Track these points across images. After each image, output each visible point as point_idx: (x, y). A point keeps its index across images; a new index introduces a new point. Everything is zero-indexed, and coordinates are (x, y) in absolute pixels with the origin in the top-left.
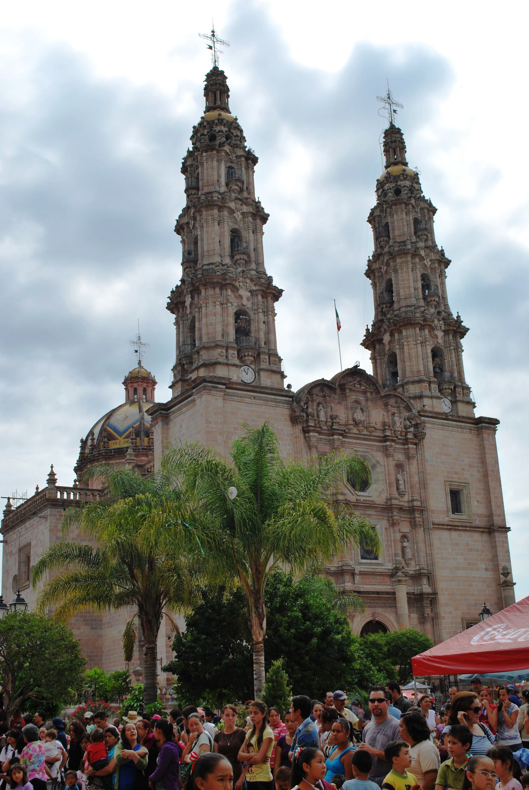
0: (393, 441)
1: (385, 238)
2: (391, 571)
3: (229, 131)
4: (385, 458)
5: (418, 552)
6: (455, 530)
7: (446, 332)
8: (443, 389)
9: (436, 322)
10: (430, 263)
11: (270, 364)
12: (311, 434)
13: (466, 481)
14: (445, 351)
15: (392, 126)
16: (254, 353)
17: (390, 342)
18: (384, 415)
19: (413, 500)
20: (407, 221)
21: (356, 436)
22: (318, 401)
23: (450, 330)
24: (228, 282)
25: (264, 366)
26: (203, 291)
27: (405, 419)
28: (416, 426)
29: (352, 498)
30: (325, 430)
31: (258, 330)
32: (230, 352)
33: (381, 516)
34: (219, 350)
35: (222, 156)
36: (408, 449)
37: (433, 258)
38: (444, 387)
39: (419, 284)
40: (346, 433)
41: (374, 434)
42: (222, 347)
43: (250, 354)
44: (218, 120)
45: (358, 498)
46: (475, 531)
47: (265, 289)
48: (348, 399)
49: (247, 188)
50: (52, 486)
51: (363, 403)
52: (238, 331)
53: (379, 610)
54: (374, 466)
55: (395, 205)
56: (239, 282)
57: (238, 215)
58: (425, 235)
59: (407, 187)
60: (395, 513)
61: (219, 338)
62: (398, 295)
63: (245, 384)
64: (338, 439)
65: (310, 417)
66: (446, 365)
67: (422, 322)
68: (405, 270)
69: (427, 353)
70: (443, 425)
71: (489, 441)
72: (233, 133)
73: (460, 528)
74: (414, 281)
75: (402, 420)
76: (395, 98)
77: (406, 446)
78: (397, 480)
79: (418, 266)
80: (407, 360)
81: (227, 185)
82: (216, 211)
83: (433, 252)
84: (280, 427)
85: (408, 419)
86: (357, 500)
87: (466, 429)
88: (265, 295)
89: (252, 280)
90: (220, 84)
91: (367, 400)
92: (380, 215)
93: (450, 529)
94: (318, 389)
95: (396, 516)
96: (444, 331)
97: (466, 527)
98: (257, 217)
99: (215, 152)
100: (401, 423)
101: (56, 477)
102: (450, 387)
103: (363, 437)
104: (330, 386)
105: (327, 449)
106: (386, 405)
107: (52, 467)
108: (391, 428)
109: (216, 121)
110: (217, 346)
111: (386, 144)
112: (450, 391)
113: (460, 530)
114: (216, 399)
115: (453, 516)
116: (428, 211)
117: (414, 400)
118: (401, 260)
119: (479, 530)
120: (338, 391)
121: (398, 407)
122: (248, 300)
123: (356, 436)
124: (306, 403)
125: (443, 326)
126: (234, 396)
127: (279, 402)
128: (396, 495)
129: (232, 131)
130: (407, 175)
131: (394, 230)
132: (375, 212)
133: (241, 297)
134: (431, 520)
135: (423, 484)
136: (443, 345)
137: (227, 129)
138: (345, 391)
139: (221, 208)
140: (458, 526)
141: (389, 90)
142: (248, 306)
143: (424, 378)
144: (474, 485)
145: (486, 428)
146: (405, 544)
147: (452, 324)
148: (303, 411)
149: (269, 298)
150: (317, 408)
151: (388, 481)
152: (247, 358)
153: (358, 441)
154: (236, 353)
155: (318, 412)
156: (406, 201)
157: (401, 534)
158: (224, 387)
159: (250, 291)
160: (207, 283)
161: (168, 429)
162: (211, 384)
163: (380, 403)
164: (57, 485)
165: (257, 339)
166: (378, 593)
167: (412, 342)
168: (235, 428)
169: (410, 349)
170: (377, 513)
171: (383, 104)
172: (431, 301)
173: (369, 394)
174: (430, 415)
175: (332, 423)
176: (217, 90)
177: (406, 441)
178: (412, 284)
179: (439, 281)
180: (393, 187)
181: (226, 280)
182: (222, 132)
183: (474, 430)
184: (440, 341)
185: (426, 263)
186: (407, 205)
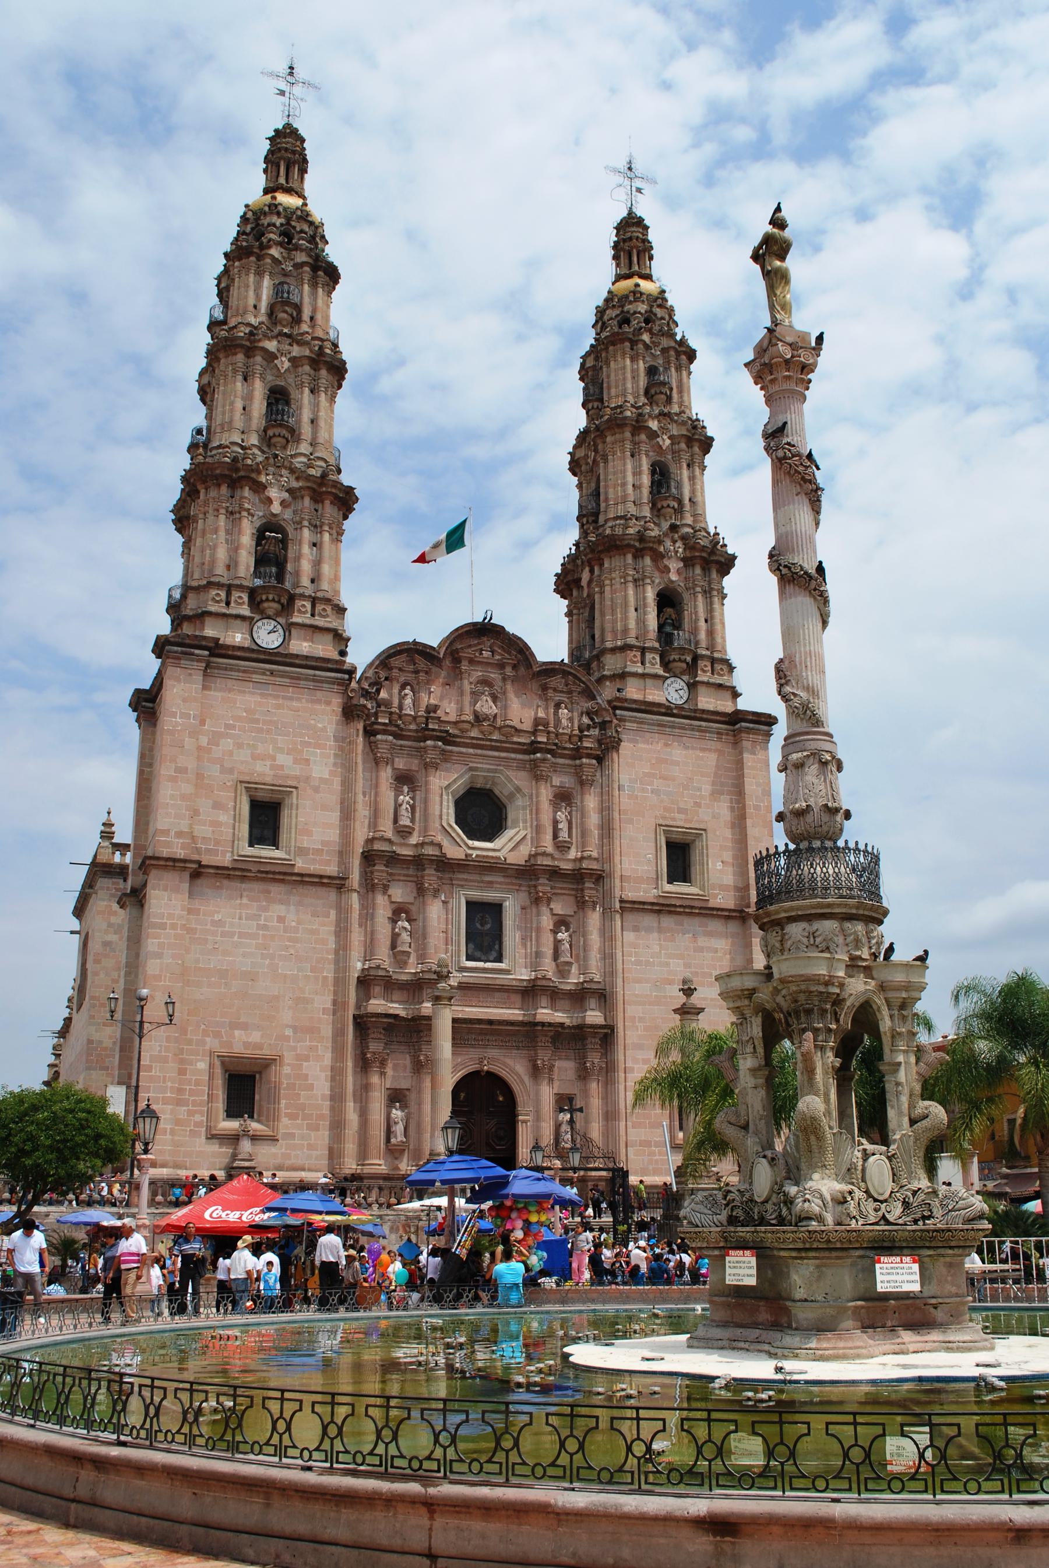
0: (549, 751)
1: (596, 404)
2: (525, 984)
3: (288, 223)
4: (534, 783)
5: (585, 950)
6: (670, 912)
7: (688, 562)
8: (669, 662)
9: (668, 543)
10: (668, 442)
11: (313, 615)
12: (379, 737)
14: (686, 596)
15: (631, 213)
16: (280, 596)
17: (590, 582)
18: (538, 706)
19: (582, 858)
20: (633, 371)
21: (475, 742)
22: (402, 679)
23: (695, 557)
24: (242, 473)
25: (297, 619)
26: (202, 492)
27: (582, 714)
28: (603, 725)
29: (454, 852)
30: (410, 730)
31: (298, 558)
32: (235, 594)
33: (513, 884)
34: (213, 592)
35: (267, 264)
37: (675, 433)
38: (672, 658)
39: (646, 480)
40: (402, 730)
41: (515, 739)
43: (271, 597)
44: (269, 206)
45: (469, 852)
46: (713, 916)
47: (314, 486)
48: (465, 675)
49: (312, 318)
50: (106, 844)
51: (498, 683)
52: (261, 561)
53: (493, 1053)
54: (511, 796)
55: (614, 344)
56: (267, 475)
57: (284, 363)
58: (661, 393)
59: (640, 313)
60: (587, 885)
61: (220, 569)
62: (607, 500)
64: (435, 747)
65: (383, 708)
66: (686, 620)
67: (637, 544)
69: (645, 598)
72: (294, 228)
73: (678, 909)
74: (634, 474)
75: (576, 714)
76: (639, 167)
77: (578, 762)
78: (555, 823)
79: (644, 447)
80: (608, 611)
81: (271, 313)
82: (240, 357)
83: (676, 422)
85: (589, 714)
87: (710, 732)
88: (317, 498)
89: (292, 470)
90: (286, 150)
91: (504, 679)
92: (594, 366)
93: (659, 912)
94: (404, 657)
95: (544, 885)
96: (683, 560)
97: (692, 907)
98: (321, 366)
99: (253, 259)
100: (571, 719)
101: (113, 829)
102: (683, 657)
103: (488, 743)
104: (429, 653)
105: (414, 764)
106: (545, 688)
107: (109, 813)
108: (552, 729)
109: (267, 209)
110: (210, 585)
111: (616, 246)
112: (684, 665)
113: (680, 913)
114: (190, 675)
115: (669, 887)
116: (678, 354)
117: (611, 682)
118: (613, 438)
119: (719, 913)
120: (447, 663)
121: (570, 692)
122: (283, 503)
123: (475, 742)
125: (680, 550)
126: (231, 670)
127: (322, 682)
128: (550, 849)
129: (293, 223)
130: (641, 294)
131: (609, 388)
132: (587, 361)
133: (269, 501)
134: (617, 893)
135: (607, 829)
136: (682, 584)
137: (283, 221)
138: (460, 662)
139: (250, 351)
140: (675, 906)
141: (631, 156)
142: (285, 517)
143: (631, 641)
145: (749, 731)
146: (560, 936)
147: (698, 546)
148: (366, 694)
149: (327, 502)
150: (400, 692)
151: (535, 823)
152: (266, 605)
153: (479, 752)
154: (245, 597)
155: (402, 698)
156: (631, 336)
157: (394, 906)
158: (206, 653)
159: (290, 491)
161: (154, 733)
162: (179, 649)
163: (534, 685)
164: (114, 841)
165: (297, 574)
166: (490, 1022)
167: (618, 579)
169: (613, 592)
170: (508, 880)
171: (620, 179)
172: (663, 507)
173: (509, 671)
174: (634, 706)
175: (427, 718)
176: (280, 158)
177: (577, 753)
178: (630, 479)
179: (685, 473)
180: (617, 316)
181: (237, 470)
182: (274, 225)
183: (727, 734)
184: (674, 577)
186: (634, 343)
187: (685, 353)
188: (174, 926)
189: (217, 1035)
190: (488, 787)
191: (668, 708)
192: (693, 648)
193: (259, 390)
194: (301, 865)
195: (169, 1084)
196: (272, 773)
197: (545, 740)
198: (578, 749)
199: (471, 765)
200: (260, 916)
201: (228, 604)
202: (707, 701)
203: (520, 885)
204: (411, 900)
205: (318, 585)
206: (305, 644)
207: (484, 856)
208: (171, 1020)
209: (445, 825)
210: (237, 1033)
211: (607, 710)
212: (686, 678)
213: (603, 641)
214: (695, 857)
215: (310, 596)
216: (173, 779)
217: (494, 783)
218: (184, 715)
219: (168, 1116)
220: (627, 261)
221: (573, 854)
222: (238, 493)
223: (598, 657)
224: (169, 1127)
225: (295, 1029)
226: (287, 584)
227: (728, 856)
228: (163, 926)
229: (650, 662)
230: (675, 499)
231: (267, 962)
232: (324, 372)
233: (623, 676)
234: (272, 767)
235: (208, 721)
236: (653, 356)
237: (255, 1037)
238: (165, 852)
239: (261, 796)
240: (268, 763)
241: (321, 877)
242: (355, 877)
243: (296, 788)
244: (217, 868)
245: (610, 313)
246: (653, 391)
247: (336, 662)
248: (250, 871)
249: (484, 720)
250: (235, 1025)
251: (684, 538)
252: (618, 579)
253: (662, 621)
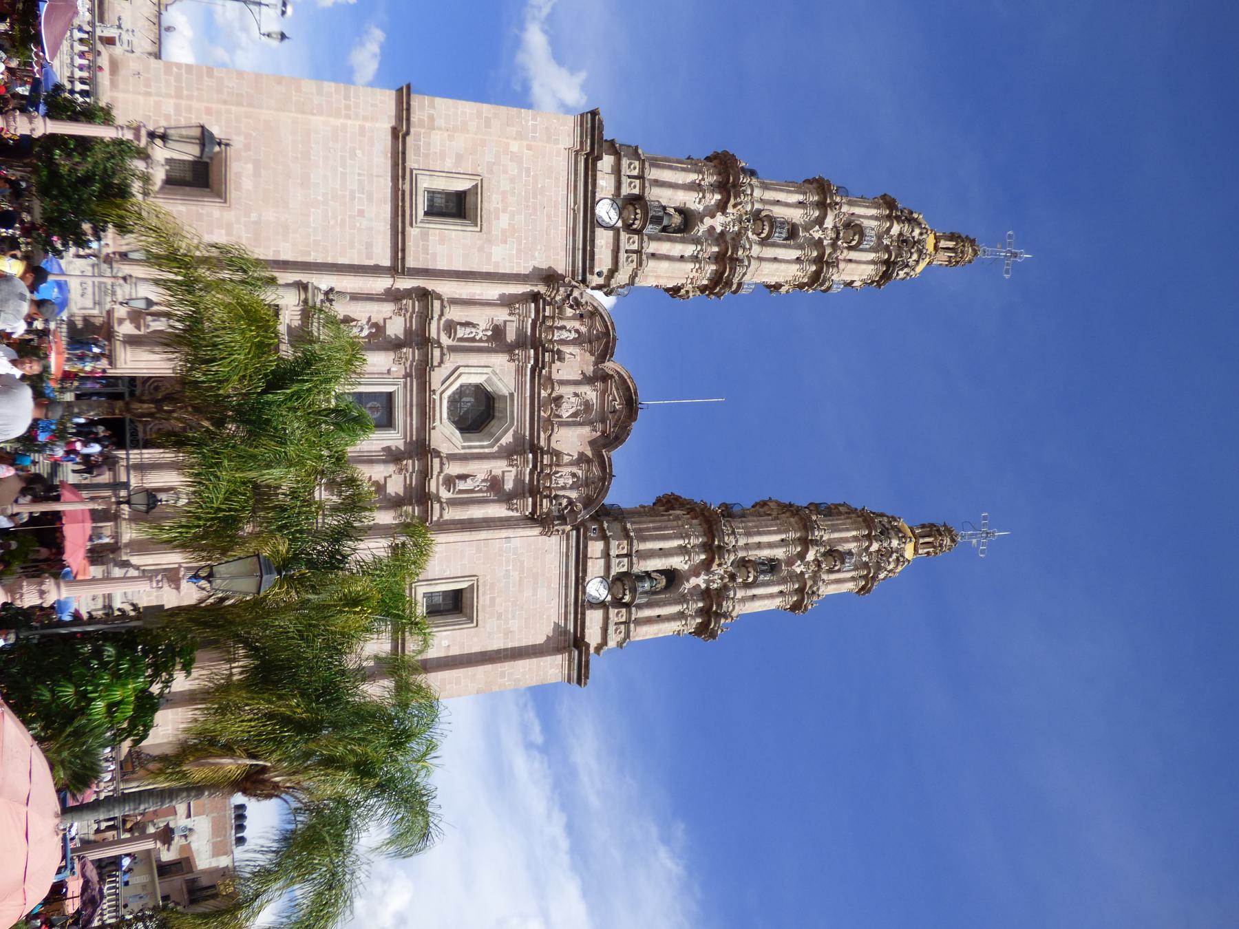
0: (535, 467)
3: (915, 242)
7: (706, 594)
8: (622, 581)
10: (798, 570)
11: (627, 251)
12: (533, 305)
19: (441, 503)
25: (624, 236)
26: (713, 164)
29: (437, 377)
39: (766, 553)
41: (542, 434)
42: (642, 169)
49: (850, 261)
55: (865, 521)
59: (890, 542)
63: (594, 203)
68: (782, 528)
71: (551, 668)
72: (913, 247)
77: (527, 495)
84: (537, 254)
86: (434, 391)
88: (719, 258)
96: (708, 588)
98: (819, 265)
100: (563, 488)
102: (627, 592)
114: (569, 135)
116: (865, 577)
122: (712, 228)
124: (577, 304)
125: (715, 586)
130: (905, 543)
131: (829, 520)
133: (713, 216)
139: (823, 206)
144: (475, 639)
147: (721, 599)
152: (631, 208)
154: (636, 191)
156: (873, 534)
160: (725, 162)
162: (589, 125)
167: (684, 531)
168: (528, 170)
172: (747, 568)
183: (565, 641)
185: (797, 564)
187: (867, 584)
188: (348, 107)
189: (247, 147)
190: (497, 414)
191: (584, 579)
192: (637, 601)
193: (796, 215)
194: (413, 233)
195: (196, 94)
196: (492, 209)
197: (545, 462)
198: (539, 492)
199: (516, 394)
200: (363, 193)
202: (594, 618)
205: (650, 258)
206: (603, 242)
207: (434, 408)
208: (264, 35)
209: (461, 370)
210: (250, 166)
211: (577, 518)
212: (609, 598)
213: (632, 523)
214: (450, 619)
215: (642, 248)
216: (479, 115)
217: (500, 419)
218: (534, 126)
219: (163, 90)
220: (923, 534)
221: (445, 494)
222: (716, 190)
223: (616, 519)
224: (152, 90)
225: (258, 223)
226: (651, 226)
227: (455, 651)
228: (347, 98)
229: (619, 563)
230: (756, 578)
231: (320, 198)
232: (814, 268)
233: (605, 538)
234: (497, 210)
235: (531, 152)
236: (860, 555)
237: (247, 184)
238: (415, 103)
239: (469, 199)
240: (500, 206)
241: (403, 250)
242: (405, 284)
243: (481, 231)
244: (404, 153)
246: (834, 554)
247: (592, 267)
248: (403, 183)
249: (556, 406)
250: (257, 163)
251: (725, 587)
252: (684, 531)
253: (654, 575)
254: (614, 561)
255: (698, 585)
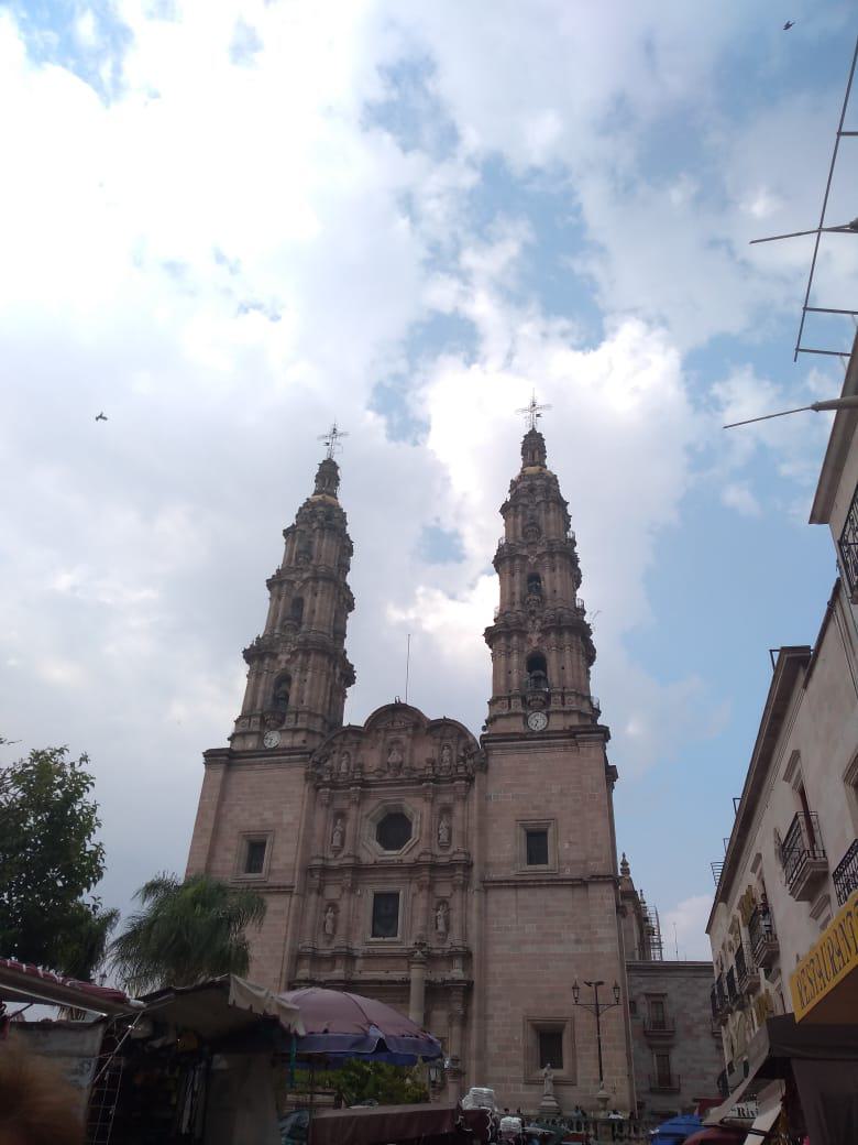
0: (433, 781)
6: (525, 887)
7: (545, 632)
13: (553, 816)
36: (455, 788)
67: (505, 630)
70: (518, 747)
88: (307, 653)
93: (516, 887)
96: (541, 631)
113: (530, 887)
145: (583, 740)
155: (340, 762)
194: (272, 881)
201: (563, 704)
203: (411, 878)
204: (337, 896)
241: (279, 887)
245: (307, 511)
254: (513, 709)
255: (539, 639)
